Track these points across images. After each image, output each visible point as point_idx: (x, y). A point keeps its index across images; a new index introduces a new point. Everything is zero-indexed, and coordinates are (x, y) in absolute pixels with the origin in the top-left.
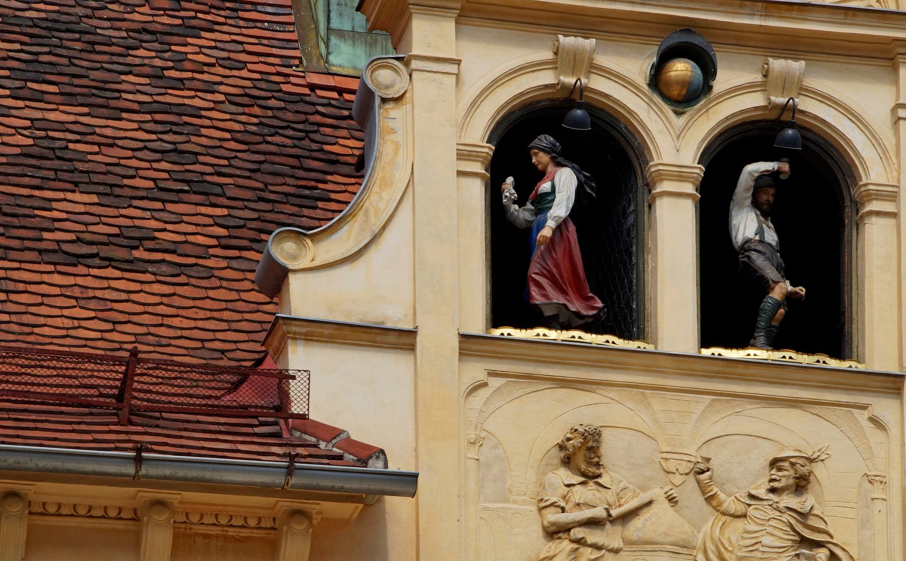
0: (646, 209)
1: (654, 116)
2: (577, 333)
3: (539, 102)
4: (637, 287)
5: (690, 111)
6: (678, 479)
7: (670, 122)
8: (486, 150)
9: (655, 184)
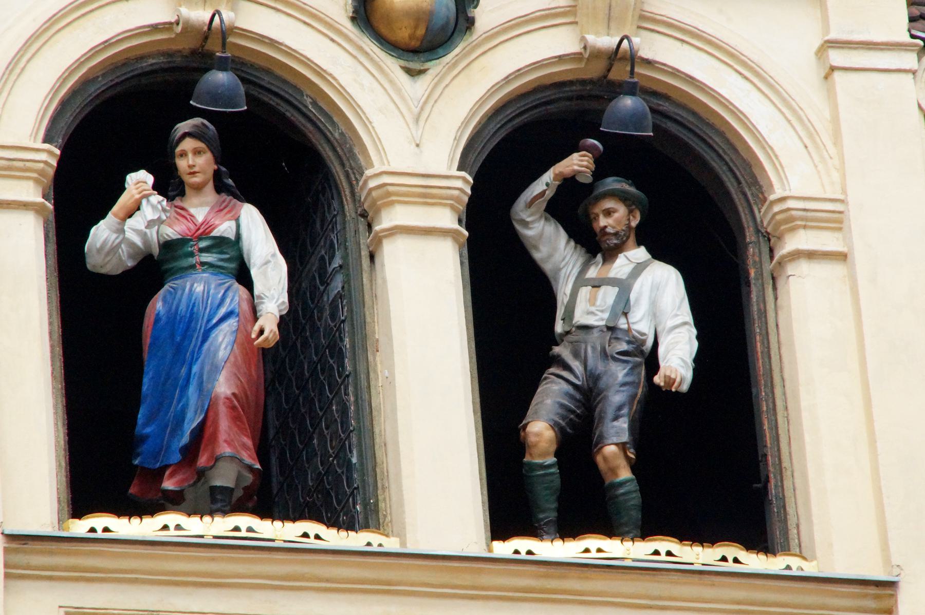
0: (366, 262)
1: (367, 79)
2: (244, 521)
3: (141, 58)
4: (358, 420)
5: (436, 68)
7: (398, 91)
8: (43, 157)
9: (378, 211)
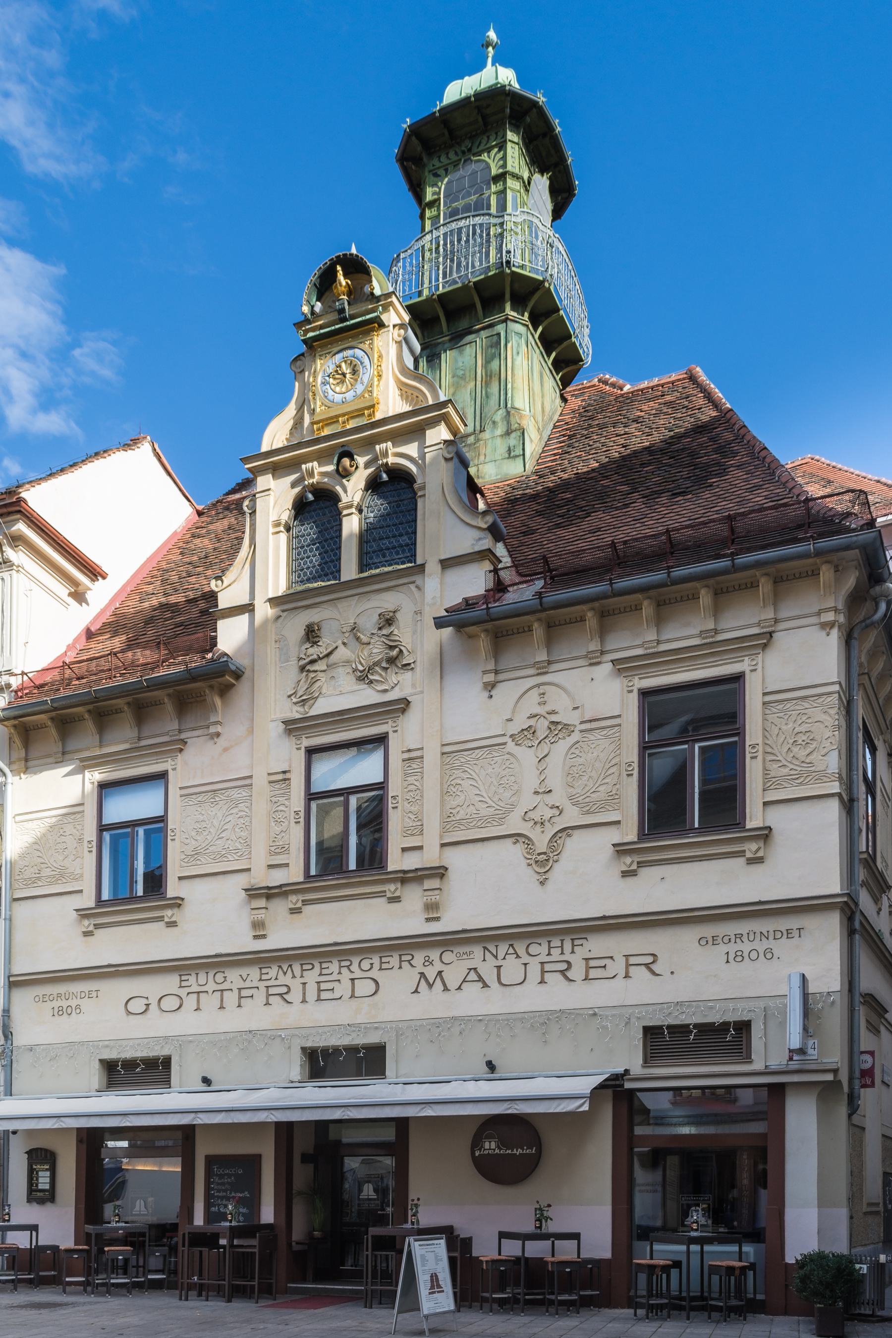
6: (347, 635)
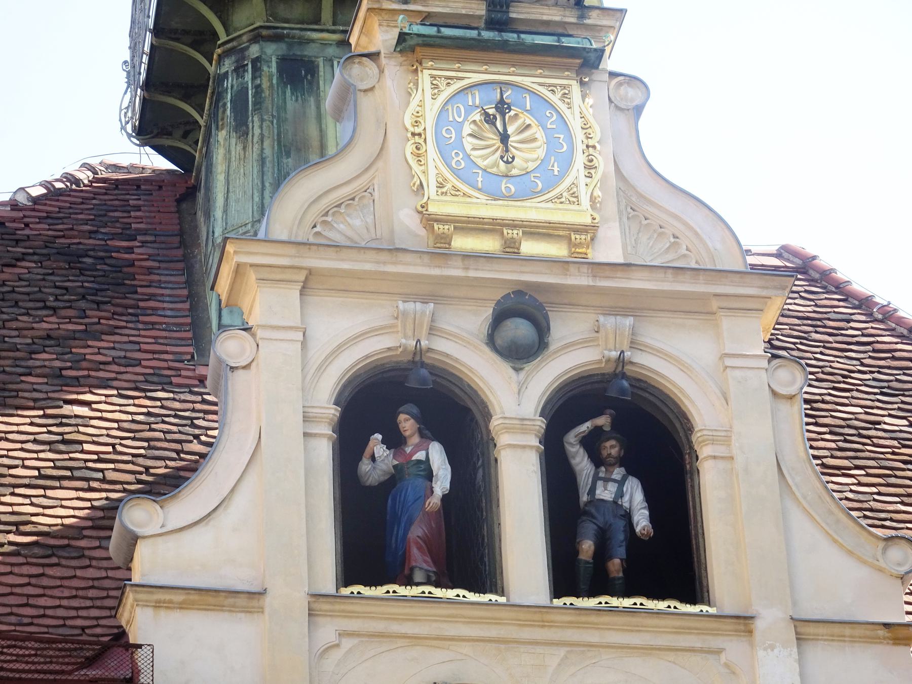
5: (528, 367)
